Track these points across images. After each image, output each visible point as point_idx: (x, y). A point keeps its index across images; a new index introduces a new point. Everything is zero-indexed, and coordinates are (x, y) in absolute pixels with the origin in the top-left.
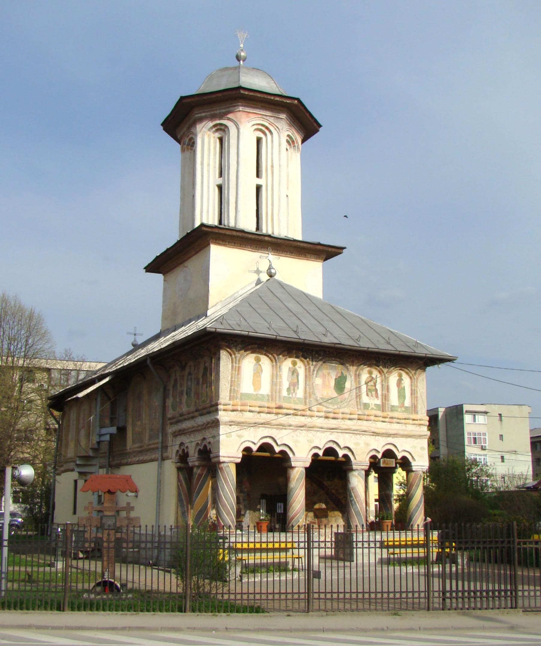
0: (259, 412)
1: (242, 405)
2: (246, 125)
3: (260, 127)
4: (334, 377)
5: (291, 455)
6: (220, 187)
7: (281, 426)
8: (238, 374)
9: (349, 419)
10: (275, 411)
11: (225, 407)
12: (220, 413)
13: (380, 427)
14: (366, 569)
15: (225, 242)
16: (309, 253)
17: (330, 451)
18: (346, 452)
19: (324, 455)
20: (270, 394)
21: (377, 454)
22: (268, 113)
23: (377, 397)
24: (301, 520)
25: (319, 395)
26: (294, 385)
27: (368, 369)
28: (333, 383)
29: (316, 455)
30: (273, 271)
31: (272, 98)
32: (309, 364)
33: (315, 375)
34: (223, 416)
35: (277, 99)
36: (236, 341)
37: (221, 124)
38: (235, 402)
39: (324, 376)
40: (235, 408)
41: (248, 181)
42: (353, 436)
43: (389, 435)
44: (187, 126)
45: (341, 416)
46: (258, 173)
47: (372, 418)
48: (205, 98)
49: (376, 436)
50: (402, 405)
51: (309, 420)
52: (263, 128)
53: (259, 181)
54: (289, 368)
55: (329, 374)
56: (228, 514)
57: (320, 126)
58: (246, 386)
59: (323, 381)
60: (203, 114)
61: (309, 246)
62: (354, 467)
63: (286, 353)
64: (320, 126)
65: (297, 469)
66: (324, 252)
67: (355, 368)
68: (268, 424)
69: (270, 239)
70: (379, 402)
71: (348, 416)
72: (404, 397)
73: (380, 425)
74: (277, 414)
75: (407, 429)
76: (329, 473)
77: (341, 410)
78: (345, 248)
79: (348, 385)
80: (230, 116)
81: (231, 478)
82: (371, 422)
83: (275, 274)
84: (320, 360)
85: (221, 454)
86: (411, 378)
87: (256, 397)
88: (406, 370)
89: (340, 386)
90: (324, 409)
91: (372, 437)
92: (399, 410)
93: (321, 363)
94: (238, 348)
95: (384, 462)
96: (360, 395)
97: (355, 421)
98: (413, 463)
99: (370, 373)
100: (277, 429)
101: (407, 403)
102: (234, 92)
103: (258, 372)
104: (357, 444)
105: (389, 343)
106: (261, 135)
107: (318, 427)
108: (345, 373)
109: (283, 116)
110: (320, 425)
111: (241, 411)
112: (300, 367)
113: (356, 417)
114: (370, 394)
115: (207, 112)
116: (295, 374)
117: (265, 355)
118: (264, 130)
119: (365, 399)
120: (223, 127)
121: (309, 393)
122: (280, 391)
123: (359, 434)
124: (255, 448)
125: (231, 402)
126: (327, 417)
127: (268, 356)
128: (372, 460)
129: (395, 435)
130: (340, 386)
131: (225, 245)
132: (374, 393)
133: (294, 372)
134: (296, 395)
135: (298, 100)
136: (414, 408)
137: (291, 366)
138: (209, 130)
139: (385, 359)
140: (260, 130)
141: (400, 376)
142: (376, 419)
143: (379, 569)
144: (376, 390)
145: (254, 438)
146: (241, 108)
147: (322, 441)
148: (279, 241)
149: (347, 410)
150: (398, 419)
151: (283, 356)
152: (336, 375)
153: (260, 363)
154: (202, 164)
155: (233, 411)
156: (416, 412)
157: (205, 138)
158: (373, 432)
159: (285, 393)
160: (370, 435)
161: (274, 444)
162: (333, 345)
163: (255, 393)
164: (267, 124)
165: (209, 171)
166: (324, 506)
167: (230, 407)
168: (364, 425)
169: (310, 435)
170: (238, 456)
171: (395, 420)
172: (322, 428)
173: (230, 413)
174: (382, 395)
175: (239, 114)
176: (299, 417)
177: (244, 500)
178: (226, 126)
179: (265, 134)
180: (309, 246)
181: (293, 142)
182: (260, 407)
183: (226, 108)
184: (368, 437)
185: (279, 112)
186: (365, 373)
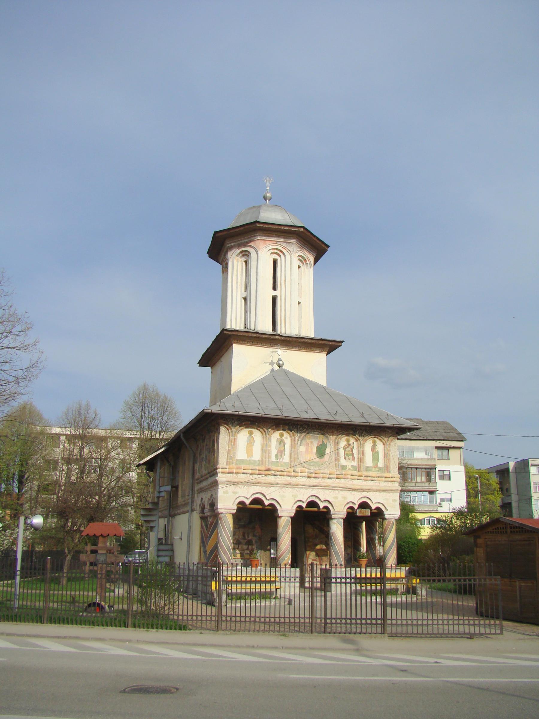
0: (251, 474)
1: (237, 469)
2: (264, 250)
3: (275, 251)
4: (316, 445)
5: (278, 507)
6: (245, 299)
7: (270, 485)
8: (234, 445)
9: (329, 478)
10: (264, 472)
11: (223, 470)
12: (219, 475)
13: (356, 484)
14: (339, 598)
15: (245, 341)
16: (314, 347)
17: (312, 504)
18: (327, 504)
19: (307, 506)
20: (261, 459)
21: (354, 506)
22: (281, 240)
23: (353, 459)
24: (286, 559)
25: (302, 460)
26: (281, 452)
28: (315, 450)
29: (300, 507)
30: (281, 362)
31: (283, 228)
32: (294, 435)
33: (299, 444)
34: (221, 477)
35: (287, 228)
36: (233, 419)
37: (246, 251)
38: (231, 466)
39: (307, 444)
40: (230, 471)
41: (265, 293)
42: (332, 491)
43: (364, 490)
44: (223, 254)
45: (321, 475)
46: (276, 286)
47: (349, 477)
48: (231, 232)
50: (376, 466)
51: (294, 479)
52: (278, 252)
53: (275, 293)
54: (277, 439)
55: (311, 442)
56: (225, 553)
57: (328, 247)
58: (241, 454)
59: (306, 448)
60: (232, 244)
61: (313, 341)
62: (333, 516)
63: (275, 427)
64: (328, 247)
65: (283, 518)
66: (328, 346)
67: (335, 437)
68: (258, 483)
69: (280, 338)
70: (355, 464)
71: (328, 476)
72: (378, 460)
73: (356, 482)
74: (266, 475)
75: (381, 485)
76: (312, 521)
77: (321, 471)
78: (343, 342)
79: (328, 451)
80: (251, 244)
81: (228, 526)
83: (283, 365)
84: (304, 432)
85: (219, 507)
86: (384, 444)
87: (249, 462)
88: (379, 437)
89: (321, 452)
90: (307, 470)
92: (373, 470)
93: (304, 434)
94: (235, 424)
95: (360, 512)
96: (338, 459)
97: (334, 480)
98: (386, 513)
99: (348, 441)
100: (266, 487)
101: (381, 464)
102: (252, 226)
103: (250, 443)
104: (336, 498)
105: (363, 417)
106: (276, 257)
107: (301, 485)
108: (325, 441)
109: (294, 241)
110: (303, 483)
111: (236, 473)
112: (286, 438)
113: (335, 476)
114: (347, 458)
115: (235, 242)
116: (282, 444)
117: (257, 429)
118: (280, 252)
119: (343, 462)
120: (247, 253)
121: (294, 457)
122: (269, 457)
123: (338, 490)
124: (248, 502)
125: (228, 467)
126: (309, 477)
127: (259, 430)
128: (350, 510)
129: (369, 490)
130: (321, 452)
131: (245, 344)
132: (351, 457)
133: (281, 442)
134: (283, 460)
135: (304, 228)
136: (387, 468)
137: (279, 437)
138: (237, 256)
139: (361, 429)
140: (276, 253)
141: (374, 442)
142: (353, 477)
143: (353, 598)
144: (353, 455)
145: (247, 494)
146: (259, 238)
147: (304, 496)
148: (288, 339)
149: (326, 471)
151: (272, 429)
152: (318, 444)
153: (253, 436)
154: (232, 282)
155: (229, 473)
156: (389, 471)
157: (235, 260)
159: (273, 459)
161: (263, 499)
162: (311, 420)
163: (248, 459)
164: (280, 248)
165: (237, 288)
166: (324, 547)
167: (227, 470)
168: (342, 483)
169: (295, 491)
170: (234, 508)
171: (369, 478)
172: (304, 486)
173: (227, 474)
174: (358, 459)
175: (257, 242)
176: (285, 477)
177: (256, 542)
178: (249, 252)
179: (280, 256)
180: (313, 341)
181: (305, 260)
182: (251, 469)
183: (248, 238)
184: (346, 492)
185: (290, 238)
186: (343, 441)
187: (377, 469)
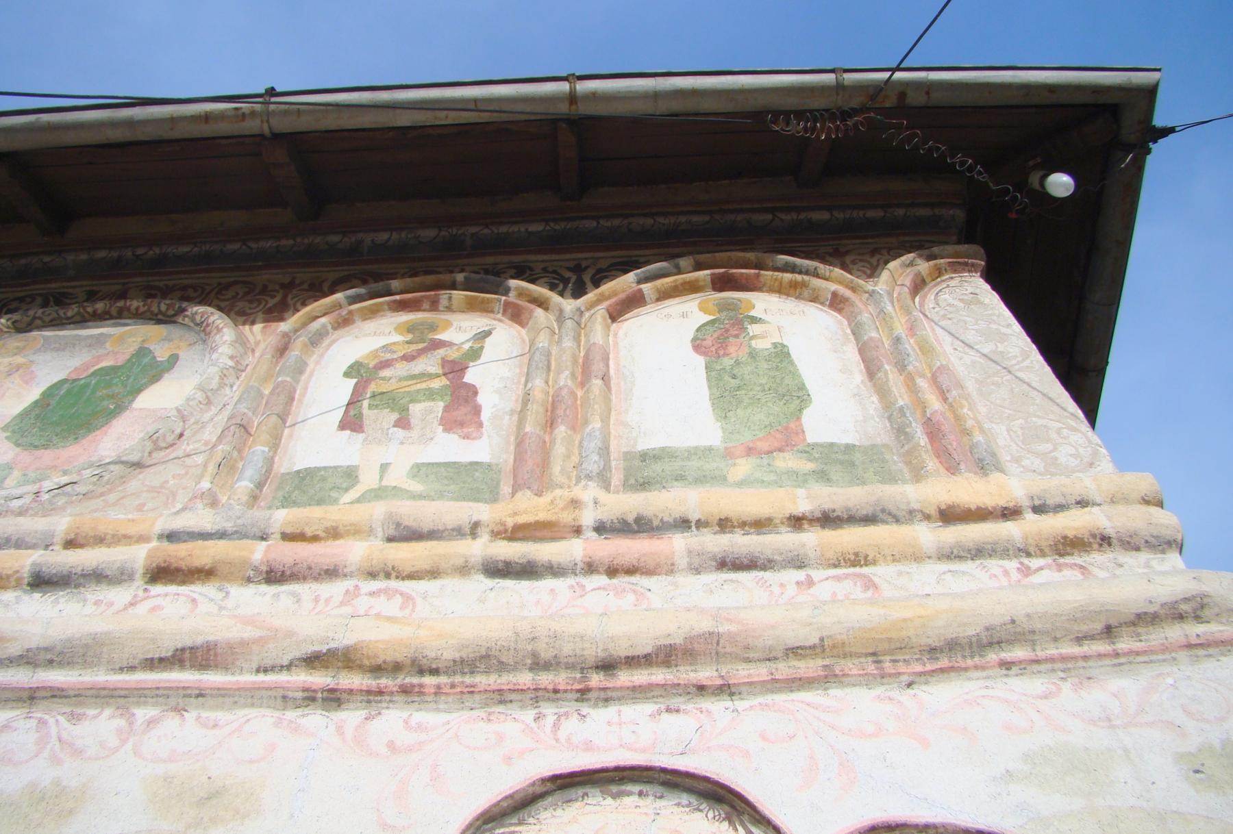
27: (405, 317)
49: (373, 696)
82: (334, 590)
91: (315, 719)
113: (139, 556)
142: (405, 554)
150: (724, 525)
158: (313, 661)
160: (285, 700)
171: (679, 543)
184: (262, 724)
187: (787, 461)
